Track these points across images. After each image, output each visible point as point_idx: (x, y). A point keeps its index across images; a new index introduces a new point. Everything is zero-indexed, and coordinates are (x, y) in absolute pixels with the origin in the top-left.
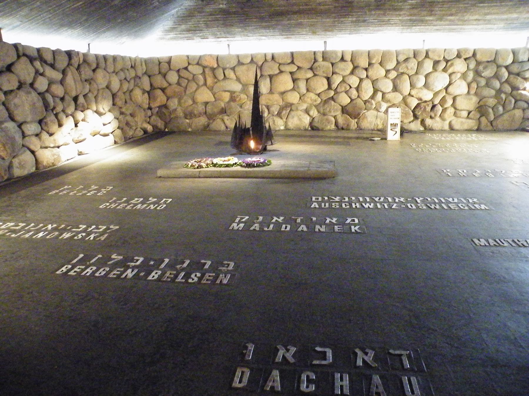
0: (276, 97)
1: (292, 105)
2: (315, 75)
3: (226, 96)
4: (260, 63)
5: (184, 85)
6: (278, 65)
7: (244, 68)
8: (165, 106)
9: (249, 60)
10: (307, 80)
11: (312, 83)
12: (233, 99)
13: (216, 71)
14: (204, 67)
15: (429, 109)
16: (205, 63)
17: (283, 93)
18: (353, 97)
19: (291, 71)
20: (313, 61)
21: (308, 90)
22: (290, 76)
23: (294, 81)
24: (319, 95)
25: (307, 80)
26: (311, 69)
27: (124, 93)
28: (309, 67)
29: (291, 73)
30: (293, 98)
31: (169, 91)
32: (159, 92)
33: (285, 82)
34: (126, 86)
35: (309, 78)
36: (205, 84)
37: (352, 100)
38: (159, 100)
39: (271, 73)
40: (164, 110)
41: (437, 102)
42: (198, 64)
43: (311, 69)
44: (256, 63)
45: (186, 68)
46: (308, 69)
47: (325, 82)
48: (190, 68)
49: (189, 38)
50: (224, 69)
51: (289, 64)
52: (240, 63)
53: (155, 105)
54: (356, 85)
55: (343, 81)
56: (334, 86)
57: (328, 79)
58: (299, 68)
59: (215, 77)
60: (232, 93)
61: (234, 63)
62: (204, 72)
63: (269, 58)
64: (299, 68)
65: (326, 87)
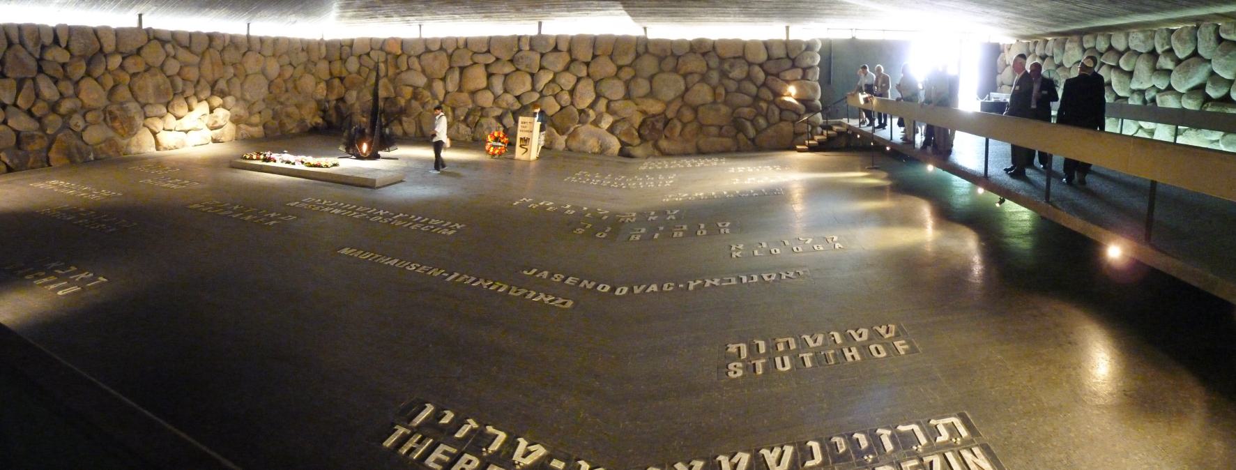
0: (464, 96)
1: (483, 108)
2: (518, 70)
3: (408, 92)
4: (450, 51)
5: (364, 75)
7: (431, 55)
8: (341, 99)
9: (437, 47)
10: (506, 75)
11: (512, 81)
12: (415, 96)
13: (400, 60)
14: (388, 53)
15: (660, 125)
16: (388, 49)
17: (473, 93)
18: (563, 103)
20: (516, 49)
21: (506, 91)
23: (490, 76)
24: (518, 98)
26: (511, 61)
27: (285, 81)
29: (487, 66)
30: (486, 99)
31: (347, 82)
32: (337, 82)
33: (477, 78)
34: (289, 72)
36: (386, 75)
37: (562, 108)
38: (336, 91)
40: (341, 104)
41: (670, 114)
42: (381, 49)
43: (511, 61)
44: (445, 51)
45: (368, 54)
47: (528, 79)
48: (372, 54)
49: (372, 17)
50: (409, 57)
52: (428, 51)
53: (333, 97)
54: (570, 88)
55: (553, 81)
56: (540, 86)
57: (532, 75)
58: (498, 59)
59: (397, 67)
60: (415, 88)
61: (421, 49)
62: (386, 62)
63: (461, 44)
64: (498, 59)
65: (528, 87)
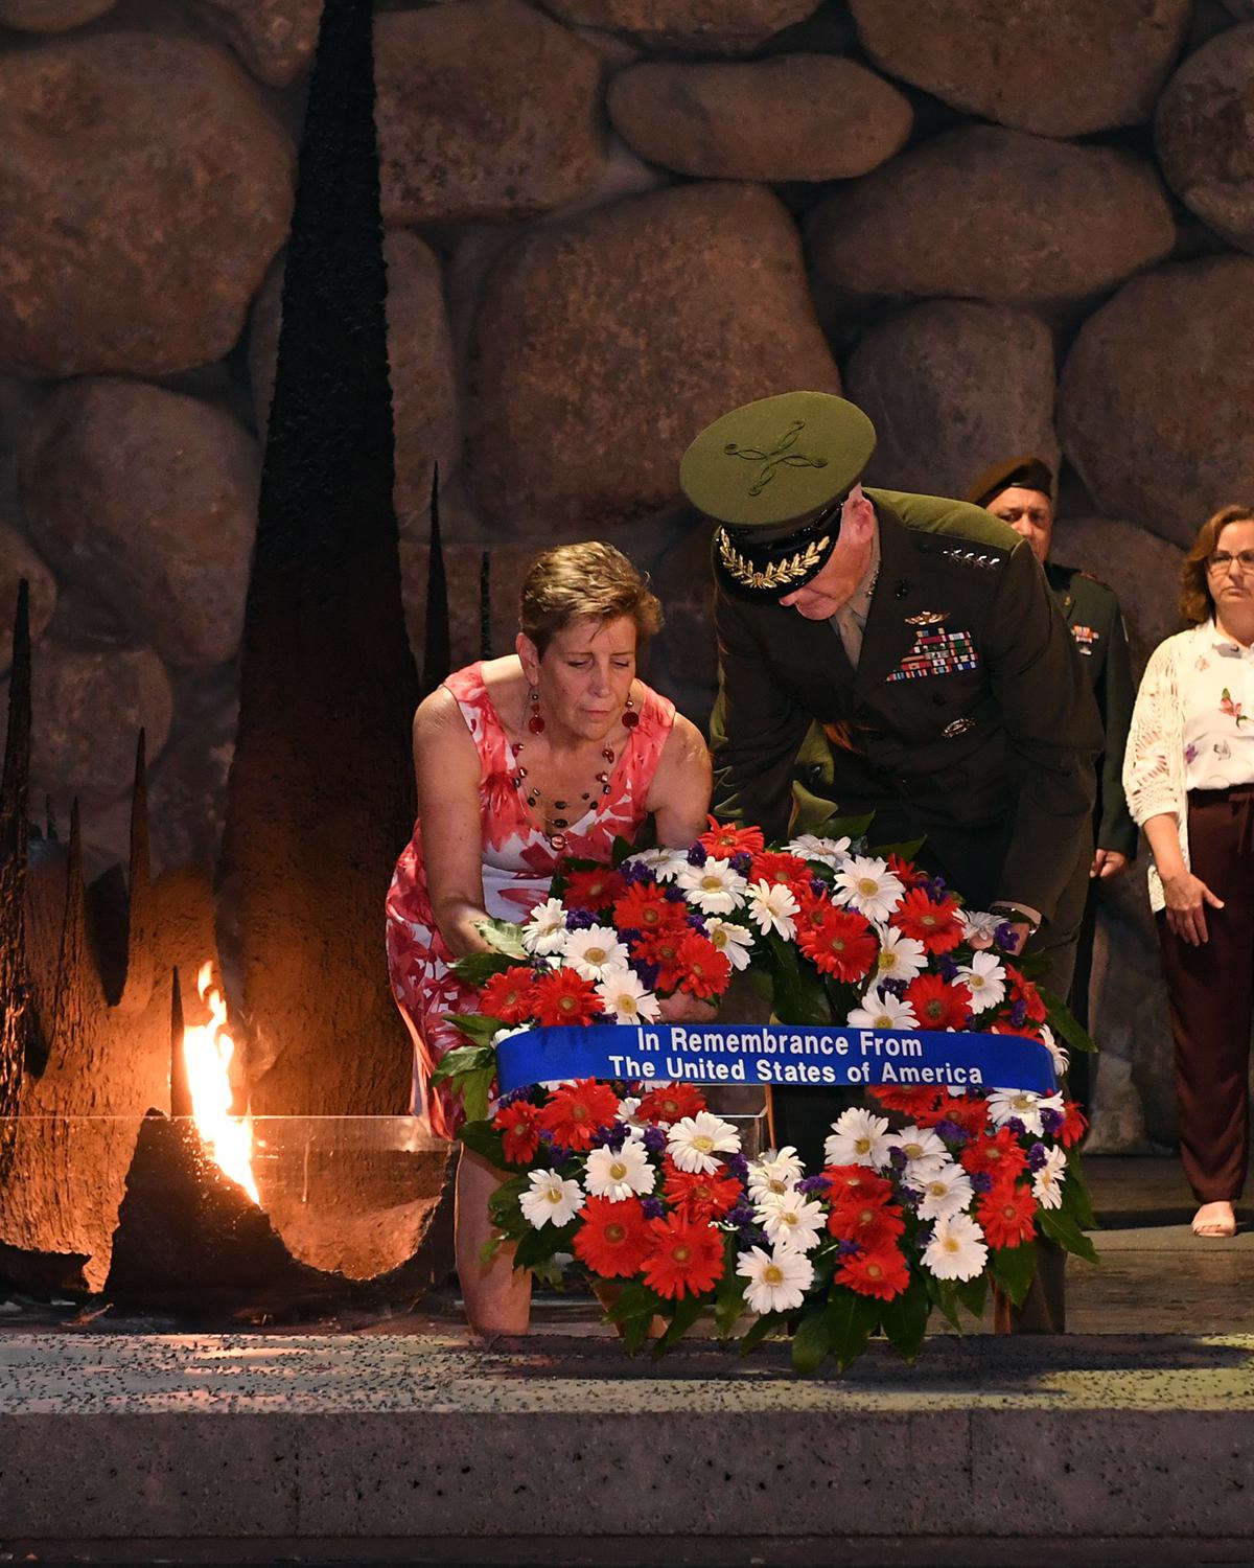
2: (1199, 246)
6: (584, 71)
10: (1069, 320)
19: (816, 168)
22: (791, 251)
25: (1069, 320)
26: (1134, 142)
28: (1106, 98)
29: (812, 208)
35: (1104, 296)
39: (476, 189)
43: (1134, 142)
46: (1091, 140)
51: (771, 50)
58: (938, 125)
64: (938, 125)
